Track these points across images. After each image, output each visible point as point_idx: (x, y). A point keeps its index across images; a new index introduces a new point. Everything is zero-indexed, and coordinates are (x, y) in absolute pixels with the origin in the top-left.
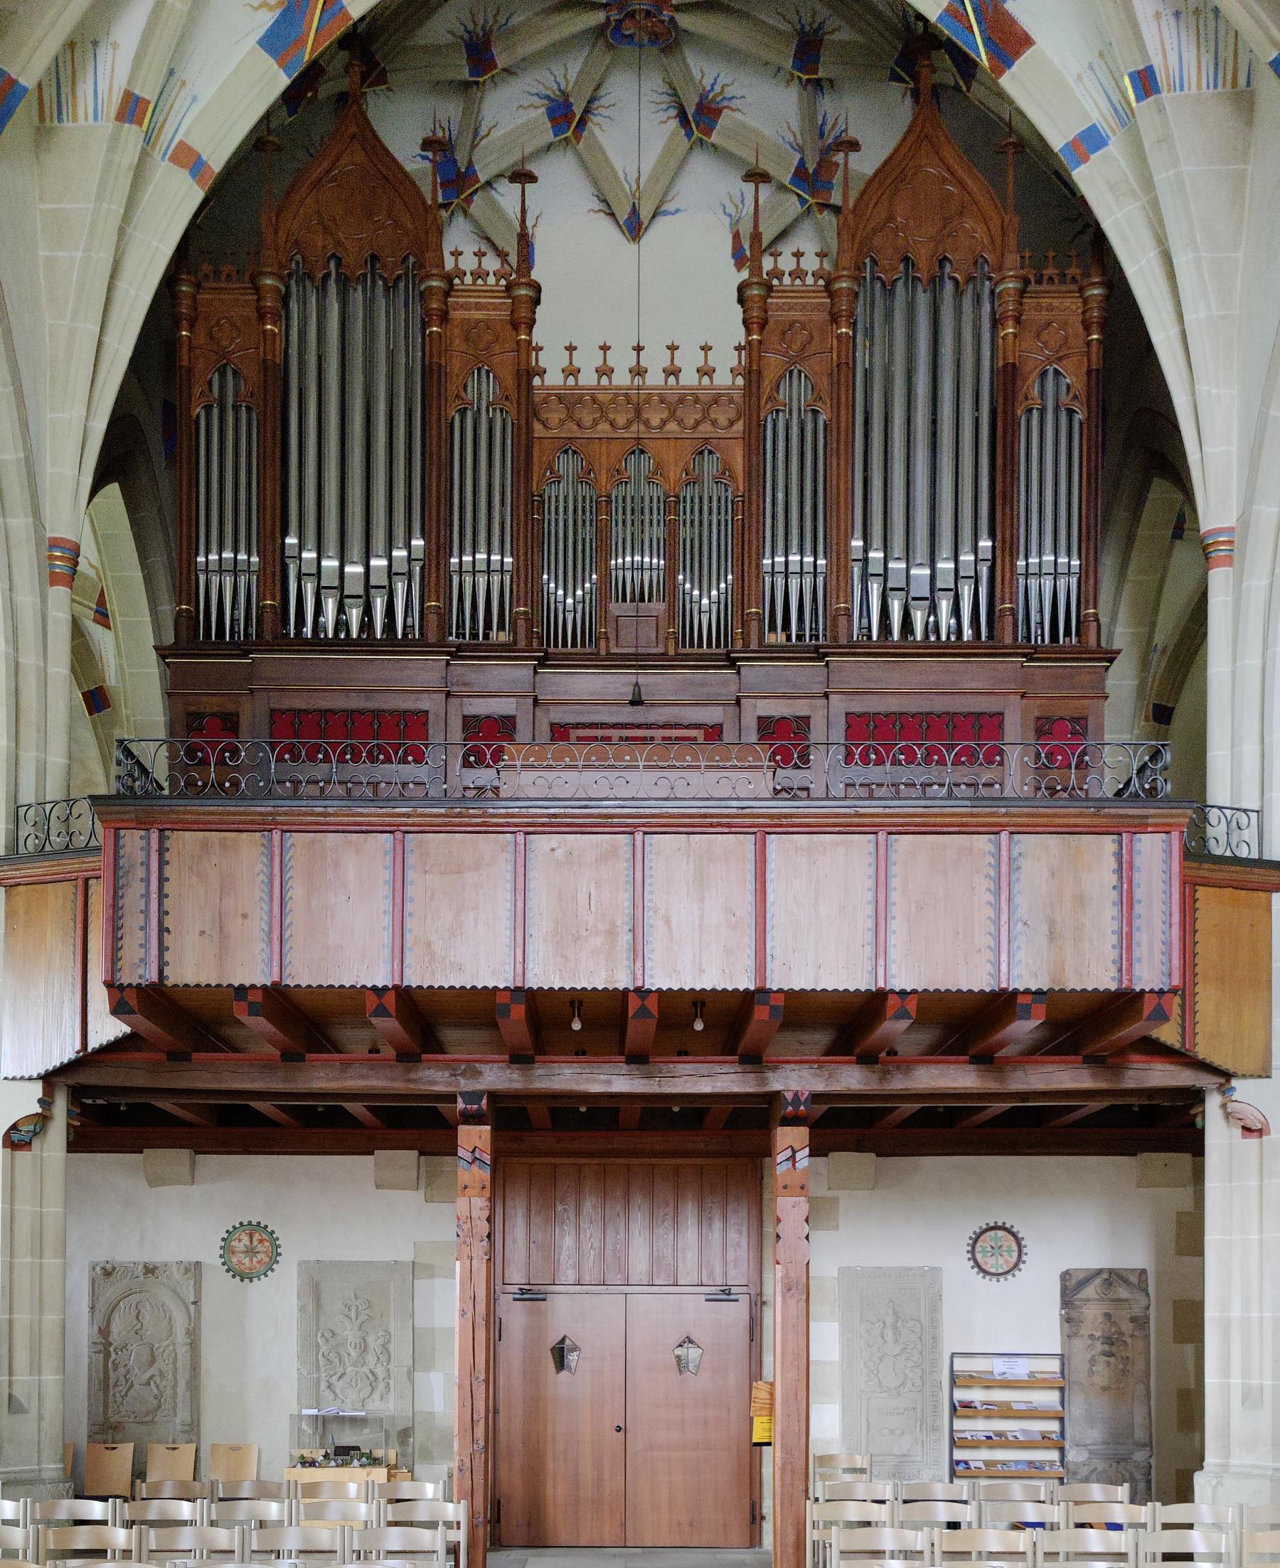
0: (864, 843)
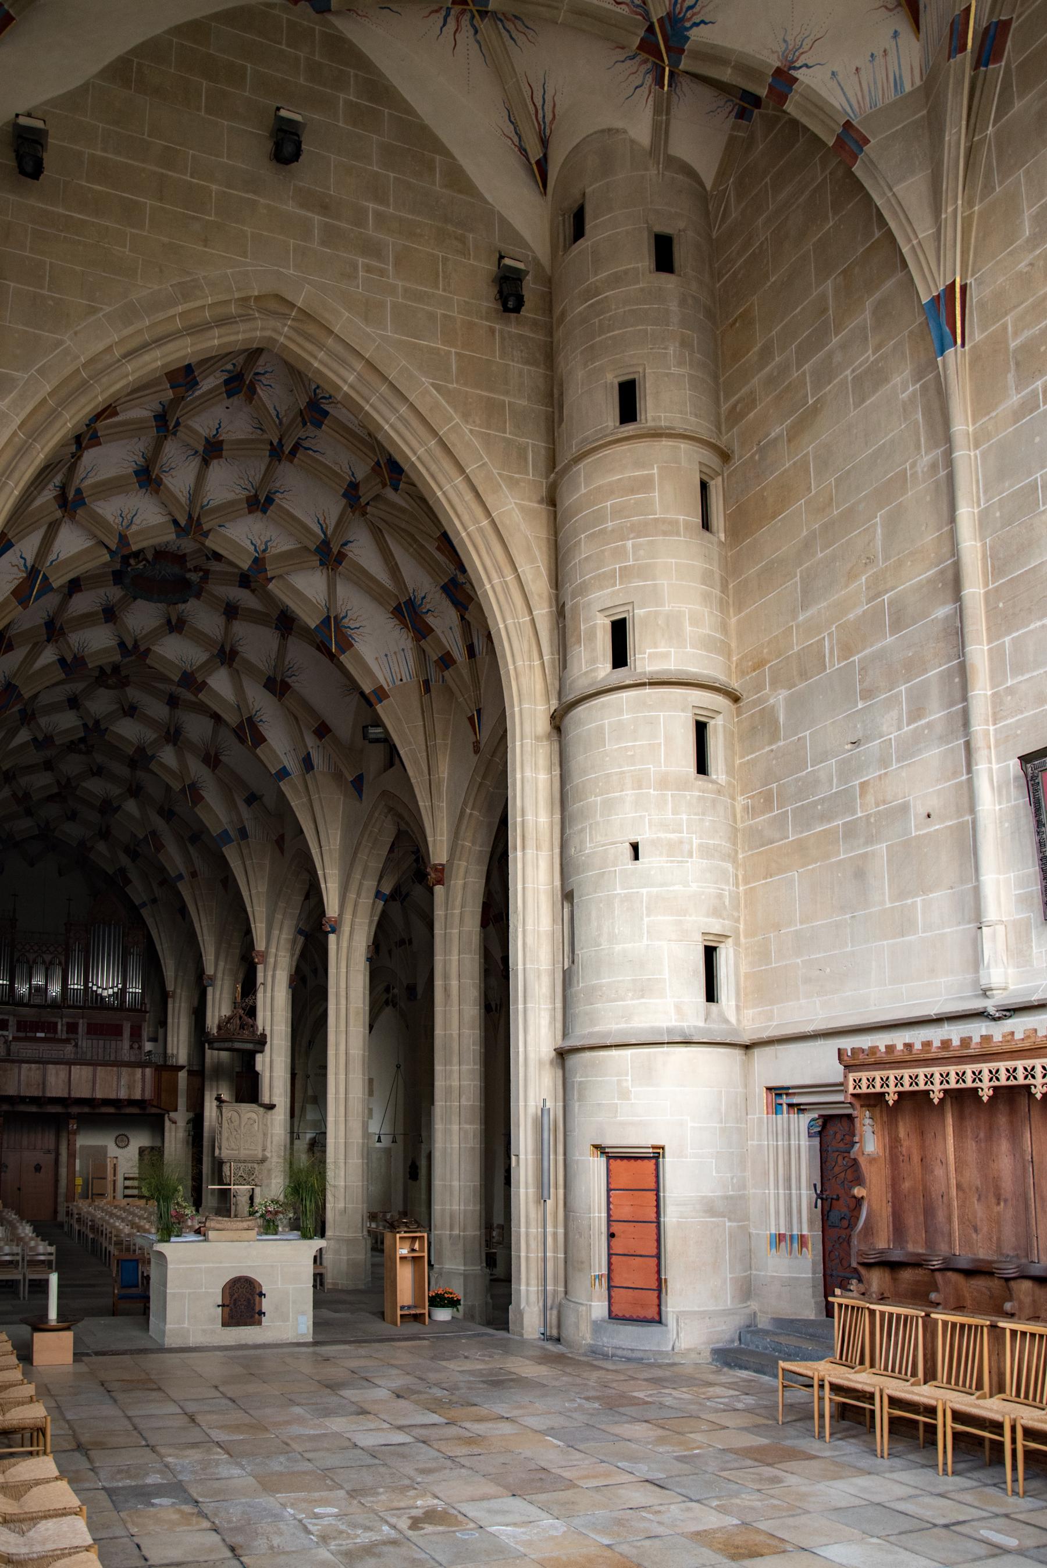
0: (91, 1068)
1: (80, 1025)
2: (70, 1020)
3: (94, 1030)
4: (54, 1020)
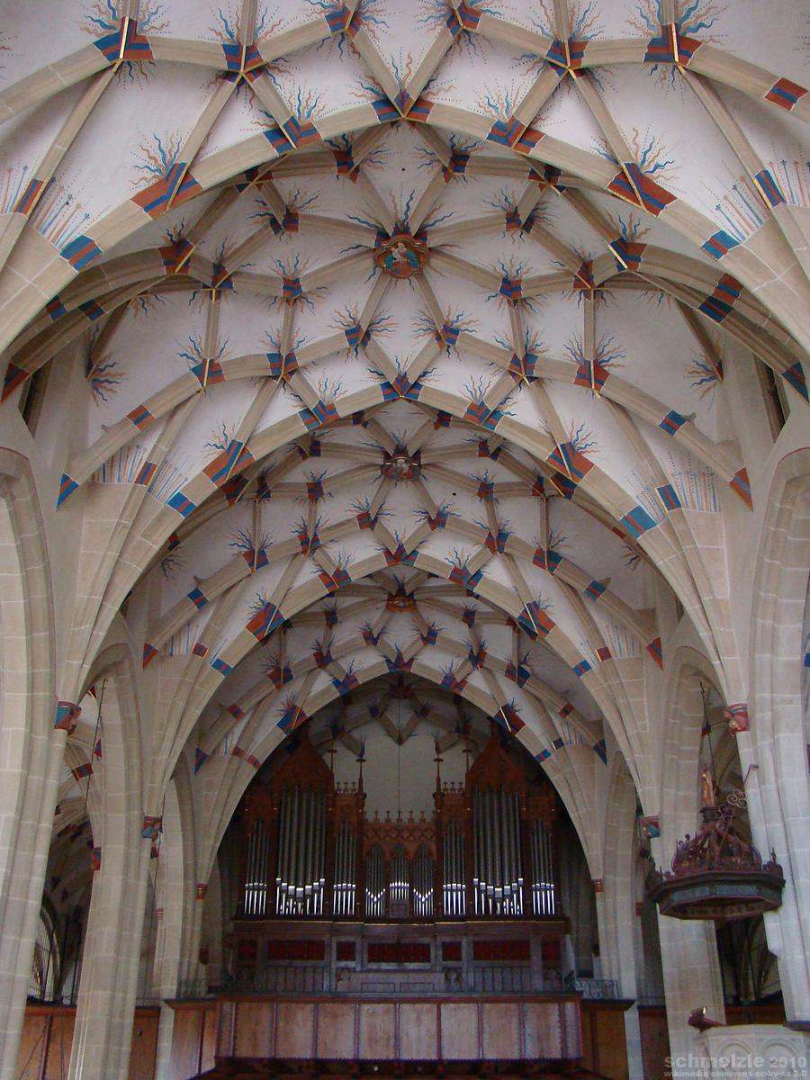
0: (473, 1007)
1: (464, 944)
2: (448, 939)
3: (484, 951)
4: (426, 940)
